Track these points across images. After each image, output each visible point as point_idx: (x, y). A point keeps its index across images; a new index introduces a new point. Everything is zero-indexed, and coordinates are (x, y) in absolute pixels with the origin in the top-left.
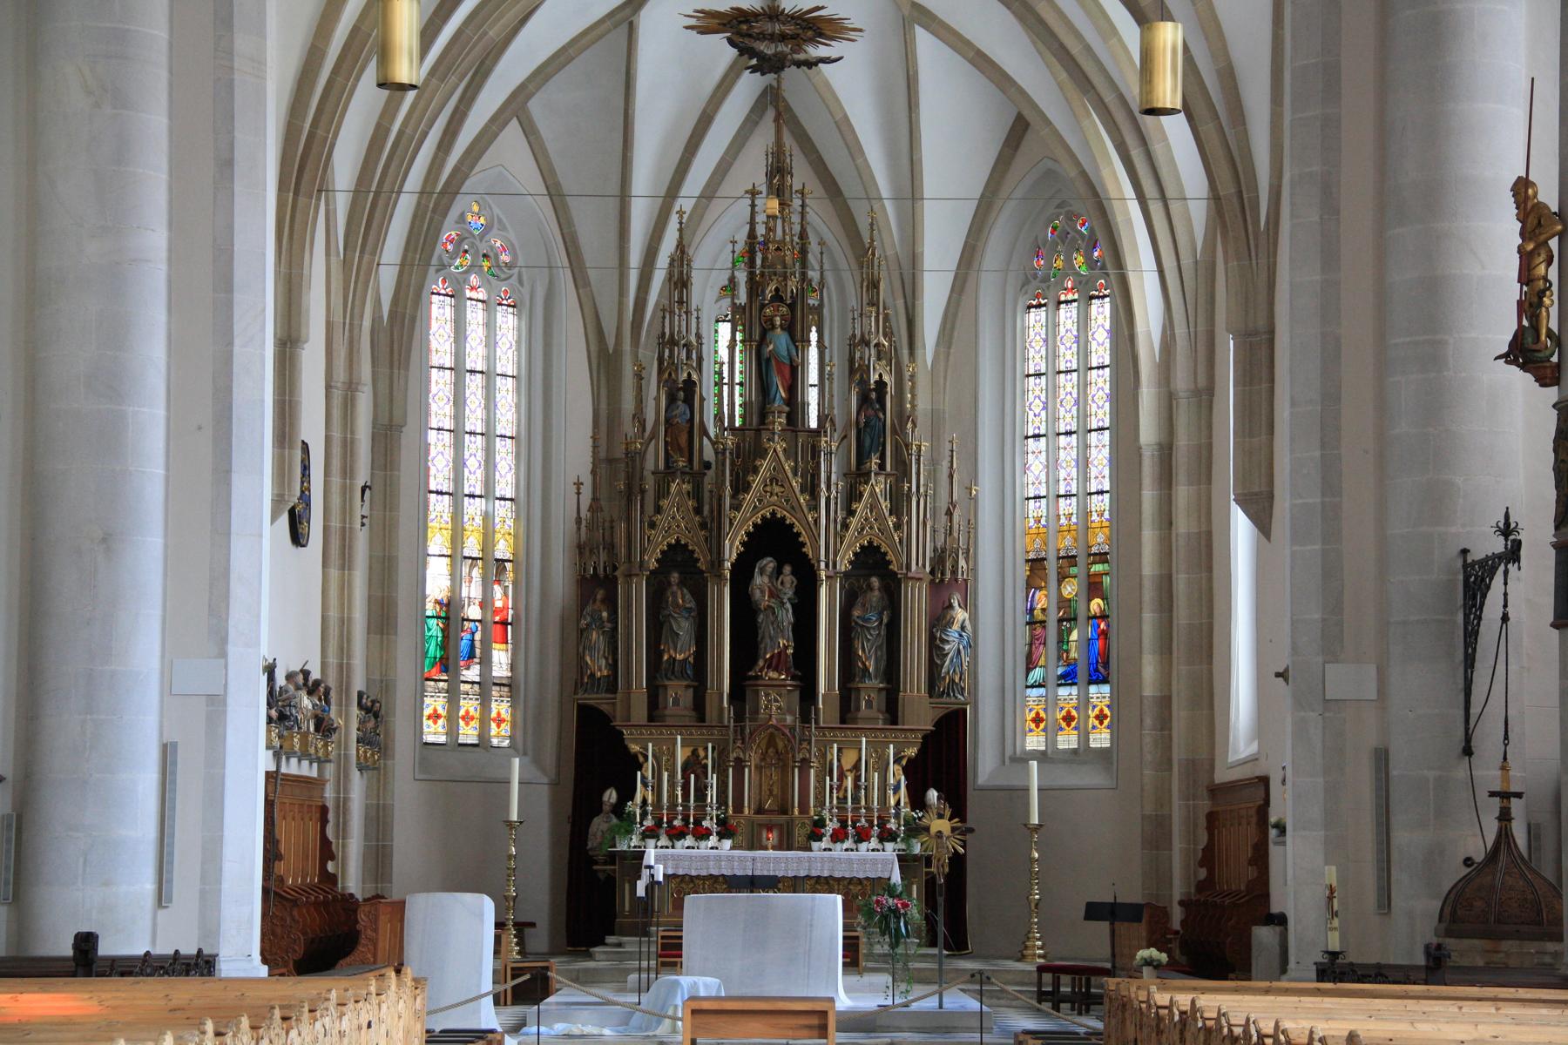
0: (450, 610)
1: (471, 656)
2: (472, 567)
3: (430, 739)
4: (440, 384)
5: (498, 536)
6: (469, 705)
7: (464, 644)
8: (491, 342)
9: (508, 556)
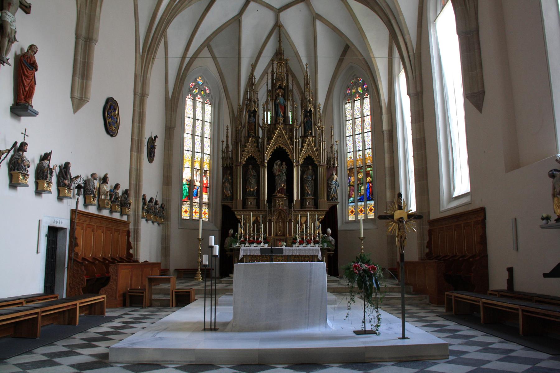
0: (191, 183)
1: (197, 195)
2: (197, 171)
3: (185, 218)
4: (188, 122)
5: (204, 164)
7: (195, 192)
8: (203, 113)
9: (208, 169)
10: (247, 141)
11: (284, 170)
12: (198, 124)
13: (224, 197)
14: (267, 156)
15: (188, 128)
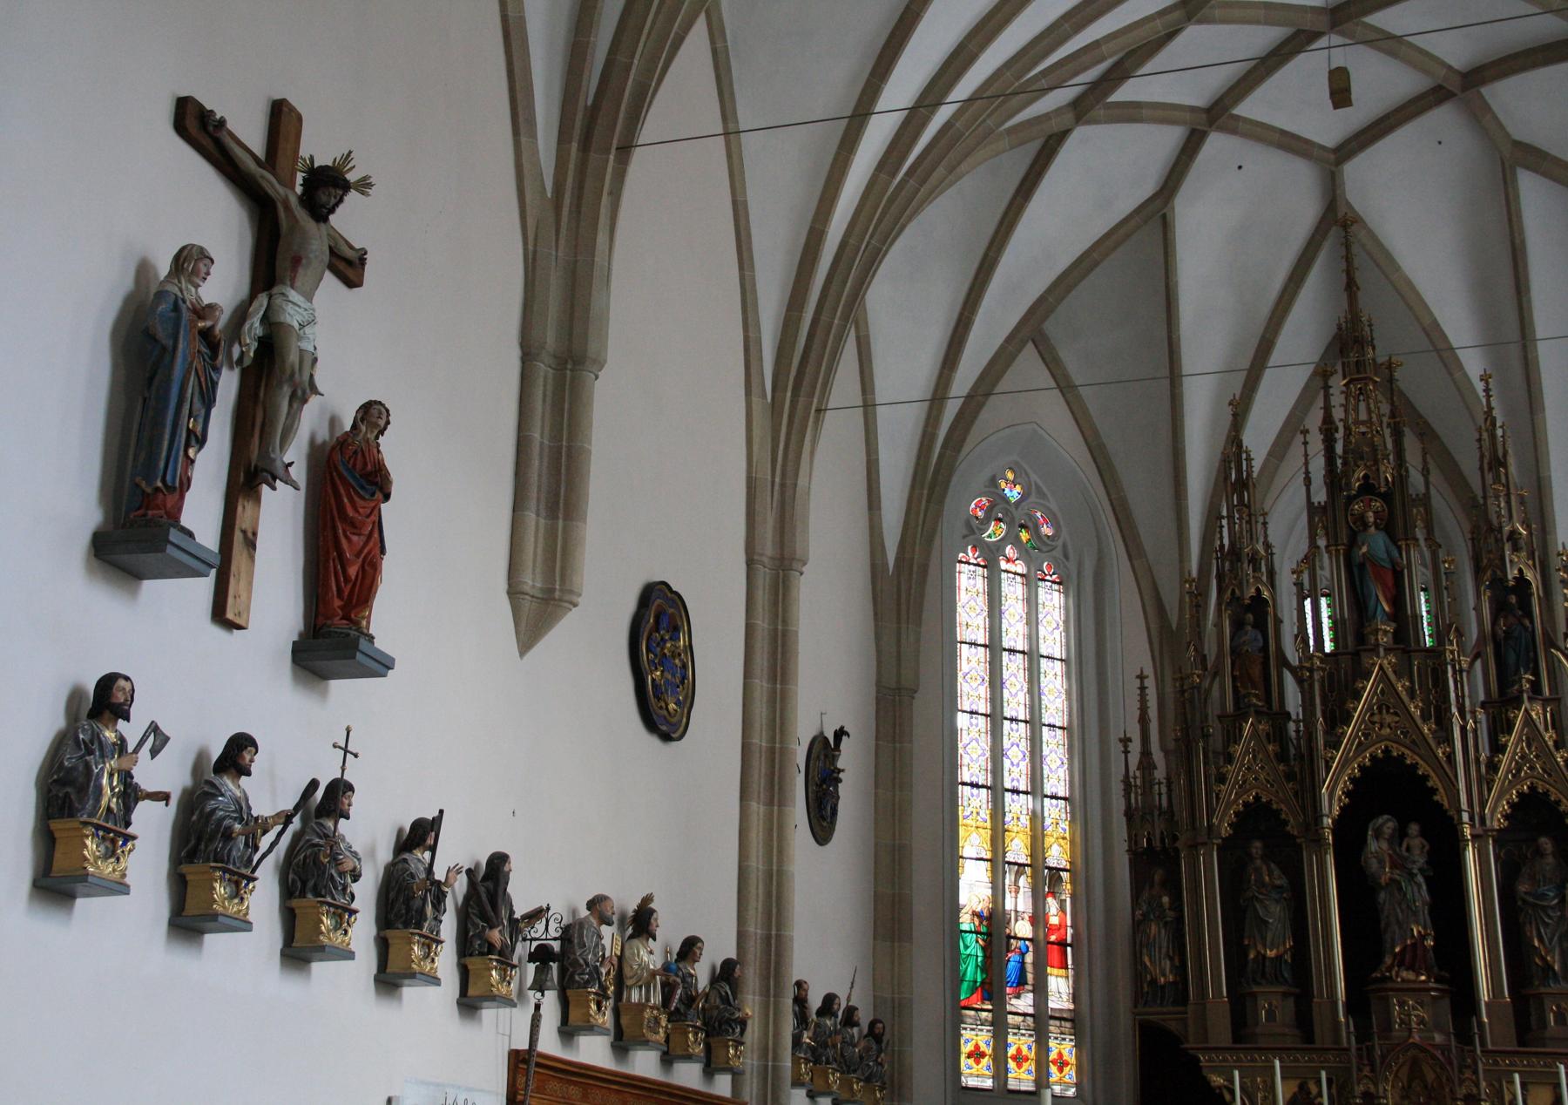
0: (994, 923)
1: (1021, 981)
2: (1018, 875)
3: (972, 1082)
4: (971, 663)
5: (1048, 841)
6: (1020, 1042)
7: (1012, 966)
8: (1032, 620)
9: (1064, 864)
10: (1233, 736)
11: (1419, 860)
12: (1013, 668)
13: (1144, 990)
14: (1332, 799)
15: (972, 690)
